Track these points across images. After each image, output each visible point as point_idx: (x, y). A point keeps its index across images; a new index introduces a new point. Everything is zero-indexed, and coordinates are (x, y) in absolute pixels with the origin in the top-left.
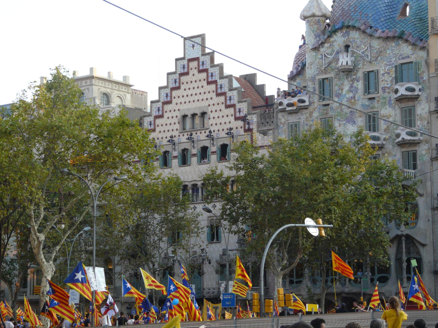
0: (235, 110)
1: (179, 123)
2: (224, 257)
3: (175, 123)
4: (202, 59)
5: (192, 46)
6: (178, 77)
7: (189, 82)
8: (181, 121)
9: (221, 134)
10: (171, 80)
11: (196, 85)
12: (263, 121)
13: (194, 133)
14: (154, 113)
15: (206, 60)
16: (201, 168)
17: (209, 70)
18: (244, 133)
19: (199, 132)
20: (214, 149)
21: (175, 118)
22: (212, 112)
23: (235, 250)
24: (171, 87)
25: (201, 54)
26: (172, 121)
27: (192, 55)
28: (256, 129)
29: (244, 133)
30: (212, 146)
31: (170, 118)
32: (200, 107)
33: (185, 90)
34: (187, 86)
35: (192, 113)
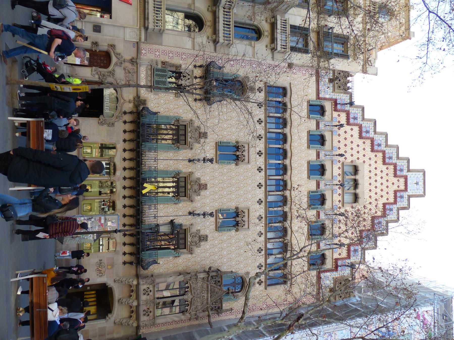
1: (352, 161)
2: (196, 239)
3: (352, 155)
4: (405, 195)
5: (418, 181)
6: (394, 162)
8: (354, 164)
10: (392, 151)
11: (384, 187)
12: (343, 283)
14: (365, 125)
17: (395, 205)
18: (334, 258)
24: (386, 151)
25: (410, 194)
26: (354, 152)
27: (410, 181)
29: (334, 258)
32: (364, 192)
34: (384, 175)
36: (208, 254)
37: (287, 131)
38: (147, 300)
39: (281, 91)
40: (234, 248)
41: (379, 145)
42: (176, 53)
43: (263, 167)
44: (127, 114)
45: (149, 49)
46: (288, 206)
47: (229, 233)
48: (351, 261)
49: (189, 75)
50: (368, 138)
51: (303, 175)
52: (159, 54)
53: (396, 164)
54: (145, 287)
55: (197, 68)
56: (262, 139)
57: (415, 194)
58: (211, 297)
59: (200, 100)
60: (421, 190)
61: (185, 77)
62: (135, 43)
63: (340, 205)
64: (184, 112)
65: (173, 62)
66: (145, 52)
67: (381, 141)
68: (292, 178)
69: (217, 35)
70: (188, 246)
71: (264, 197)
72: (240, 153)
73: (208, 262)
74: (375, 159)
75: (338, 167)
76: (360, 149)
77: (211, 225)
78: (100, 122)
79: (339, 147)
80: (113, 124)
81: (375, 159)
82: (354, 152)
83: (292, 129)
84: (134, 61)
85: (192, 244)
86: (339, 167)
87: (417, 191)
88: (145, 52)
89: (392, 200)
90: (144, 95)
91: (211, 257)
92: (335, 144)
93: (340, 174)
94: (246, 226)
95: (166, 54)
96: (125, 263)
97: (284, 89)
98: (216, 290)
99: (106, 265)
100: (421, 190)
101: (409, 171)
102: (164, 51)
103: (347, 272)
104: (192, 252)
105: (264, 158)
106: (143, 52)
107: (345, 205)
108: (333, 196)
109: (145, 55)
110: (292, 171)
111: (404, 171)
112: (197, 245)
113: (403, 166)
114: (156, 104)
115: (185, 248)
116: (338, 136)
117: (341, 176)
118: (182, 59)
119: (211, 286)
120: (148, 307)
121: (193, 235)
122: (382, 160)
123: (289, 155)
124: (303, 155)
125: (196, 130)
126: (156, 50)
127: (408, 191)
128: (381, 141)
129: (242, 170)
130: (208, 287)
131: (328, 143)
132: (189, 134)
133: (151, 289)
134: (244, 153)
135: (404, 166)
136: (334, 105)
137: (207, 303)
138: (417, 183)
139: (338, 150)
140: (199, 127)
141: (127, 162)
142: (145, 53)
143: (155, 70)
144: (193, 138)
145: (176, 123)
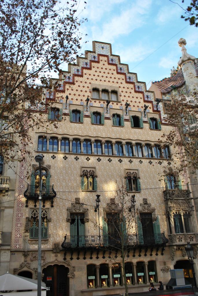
0: (144, 96)
1: (90, 92)
2: (146, 206)
4: (111, 57)
5: (101, 47)
6: (89, 62)
8: (92, 91)
9: (132, 108)
10: (82, 62)
15: (115, 59)
16: (115, 130)
18: (153, 112)
20: (127, 117)
22: (122, 92)
25: (110, 54)
26: (84, 90)
28: (163, 112)
29: (153, 112)
32: (111, 86)
36: (155, 198)
37: (71, 138)
38: (185, 239)
39: (41, 140)
41: (78, 71)
42: (17, 221)
43: (97, 157)
44: (66, 257)
45: (16, 242)
46: (122, 141)
47: (141, 184)
48: (154, 101)
49: (33, 211)
50: (74, 78)
51: (101, 128)
52: (18, 235)
53: (90, 60)
54: (177, 240)
55: (28, 205)
56: (78, 157)
57: (109, 50)
59: (52, 202)
60: (107, 46)
61: (35, 214)
62: (11, 253)
63: (119, 104)
64: (62, 215)
65: (24, 224)
66: (18, 245)
67: (75, 69)
68: (104, 137)
69: (3, 189)
71: (117, 158)
72: (89, 173)
73: (159, 198)
74: (88, 75)
75: (94, 103)
76: (81, 85)
78: (73, 277)
79: (81, 100)
80: (74, 267)
81: (88, 75)
82: (84, 90)
83: (70, 134)
84: (26, 253)
86: (95, 102)
87: (108, 49)
88: (18, 245)
89: (114, 67)
90: (51, 245)
92: (78, 103)
93: (99, 102)
94: (136, 171)
95: (19, 229)
96: (162, 254)
97: (40, 137)
98: (177, 194)
99: (164, 266)
100: (107, 46)
101: (94, 52)
102: (16, 230)
103: (161, 105)
104: (154, 209)
105: (91, 157)
106: (18, 246)
107: (119, 101)
108: (114, 108)
109: (20, 245)
110: (99, 136)
111: (95, 55)
112: (149, 205)
113: (92, 56)
114: (57, 236)
115: (151, 214)
116: (73, 100)
117: (100, 101)
118: (22, 216)
119: (175, 197)
120: (188, 238)
121: (143, 209)
122: (88, 70)
123: (88, 138)
124: (87, 127)
125: (74, 206)
126: (16, 237)
127: (108, 55)
128: (75, 69)
129: (100, 173)
130: (176, 199)
131: (79, 108)
132: (77, 211)
133: (178, 236)
134: (89, 171)
136: (51, 101)
137: (184, 200)
138: (103, 48)
139: (83, 101)
140: (72, 204)
141: (99, 256)
142: (19, 245)
143: (31, 237)
144: (80, 208)
145: (70, 221)
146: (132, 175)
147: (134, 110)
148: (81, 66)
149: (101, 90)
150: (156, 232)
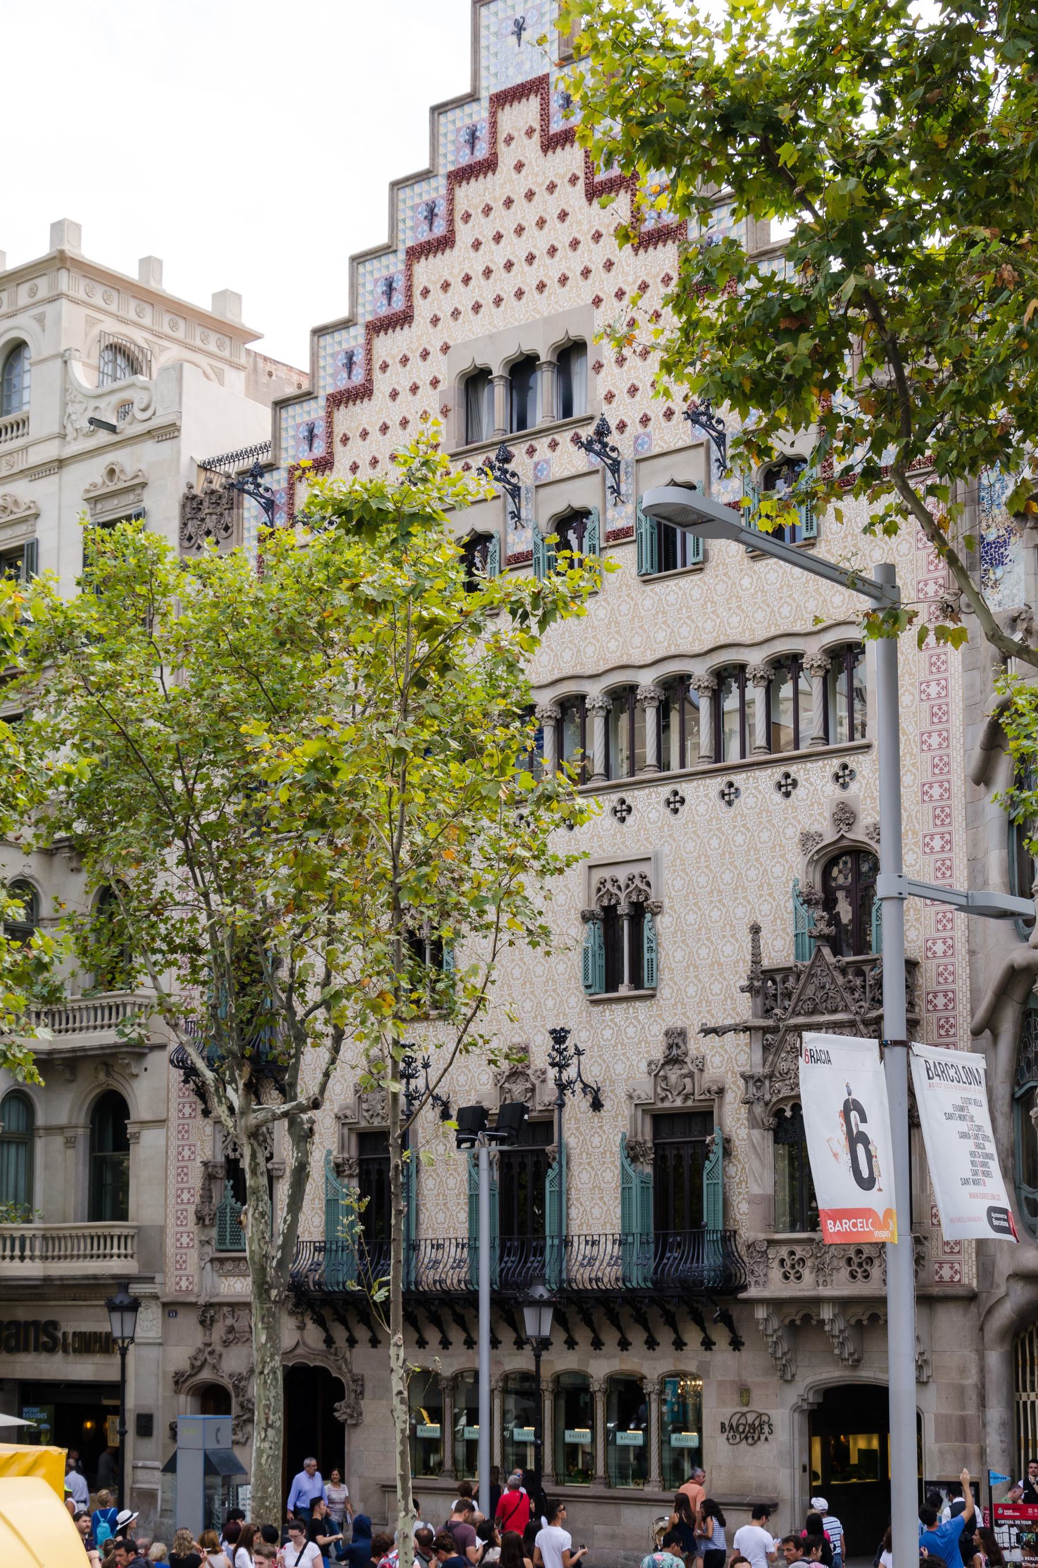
2: (674, 1074)
7: (498, 206)
9: (656, 436)
10: (409, 213)
13: (518, 451)
19: (542, 444)
20: (620, 517)
21: (425, 389)
23: (735, 1029)
30: (611, 498)
31: (405, 395)
32: (547, 321)
33: (477, 245)
35: (510, 351)
40: (715, 914)
54: (776, 1273)
58: (835, 1011)
67: (376, 281)
70: (697, 1104)
77: (636, 1018)
85: (689, 1089)
91: (739, 1010)
104: (715, 1088)
107: (589, 414)
111: (475, 118)
113: (458, 130)
120: (843, 1263)
121: (659, 1090)
135: (459, 124)
146: (622, 896)
147: (666, 449)
148: (404, 241)
149: (498, 370)
150: (711, 1217)
